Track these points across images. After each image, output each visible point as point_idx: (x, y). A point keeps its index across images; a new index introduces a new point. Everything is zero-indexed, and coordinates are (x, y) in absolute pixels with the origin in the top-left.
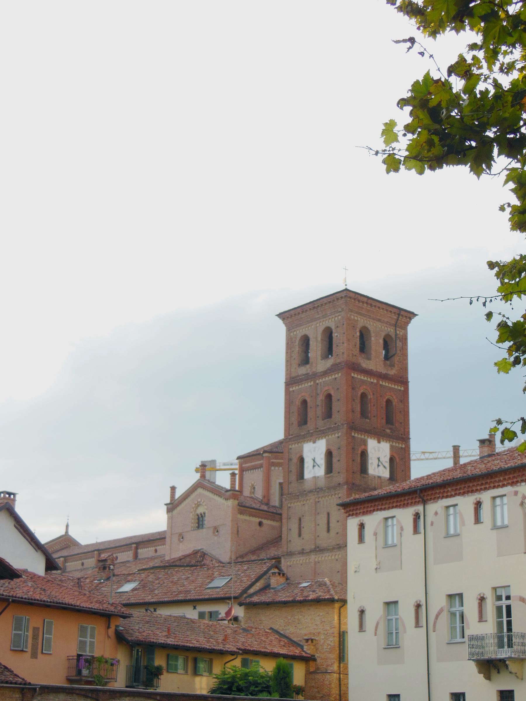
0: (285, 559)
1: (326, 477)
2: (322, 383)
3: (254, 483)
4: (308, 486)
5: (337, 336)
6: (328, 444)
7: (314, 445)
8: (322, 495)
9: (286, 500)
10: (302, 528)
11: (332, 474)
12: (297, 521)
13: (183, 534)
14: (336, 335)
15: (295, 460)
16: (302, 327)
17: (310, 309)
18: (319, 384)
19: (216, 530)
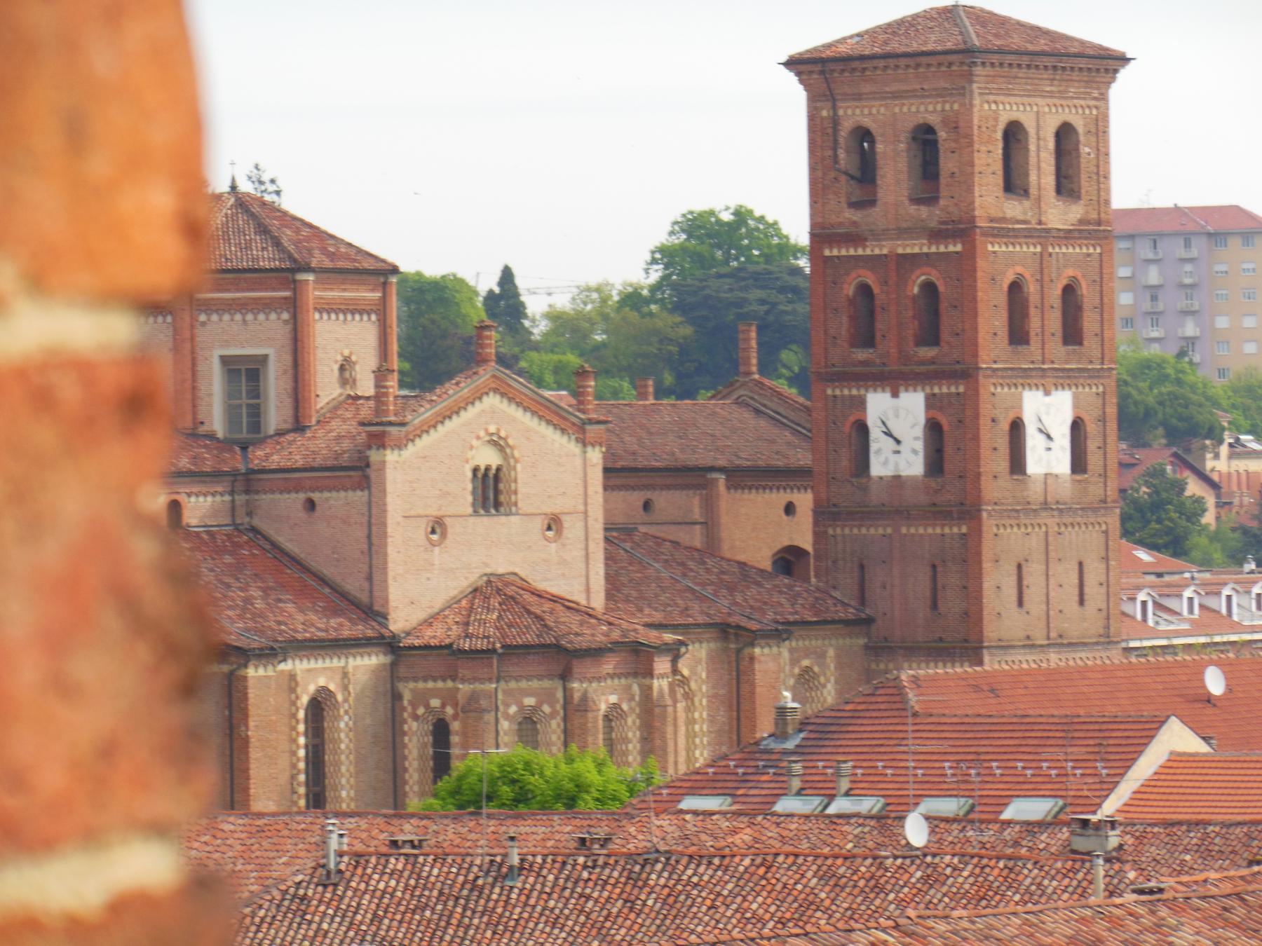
0: (991, 654)
1: (1074, 481)
2: (1061, 256)
3: (351, 353)
4: (1035, 492)
5: (1089, 154)
6: (1076, 405)
7: (1047, 399)
8: (1071, 520)
9: (990, 516)
10: (1024, 587)
11: (1086, 476)
12: (1014, 571)
13: (448, 521)
14: (1087, 150)
15: (1005, 426)
16: (1012, 99)
17: (1046, 67)
18: (1054, 256)
19: (554, 524)
